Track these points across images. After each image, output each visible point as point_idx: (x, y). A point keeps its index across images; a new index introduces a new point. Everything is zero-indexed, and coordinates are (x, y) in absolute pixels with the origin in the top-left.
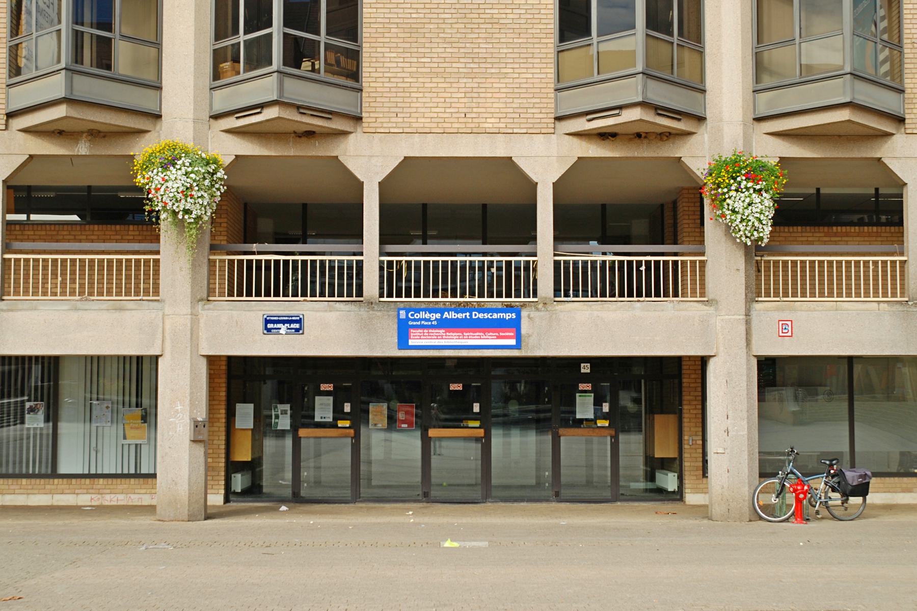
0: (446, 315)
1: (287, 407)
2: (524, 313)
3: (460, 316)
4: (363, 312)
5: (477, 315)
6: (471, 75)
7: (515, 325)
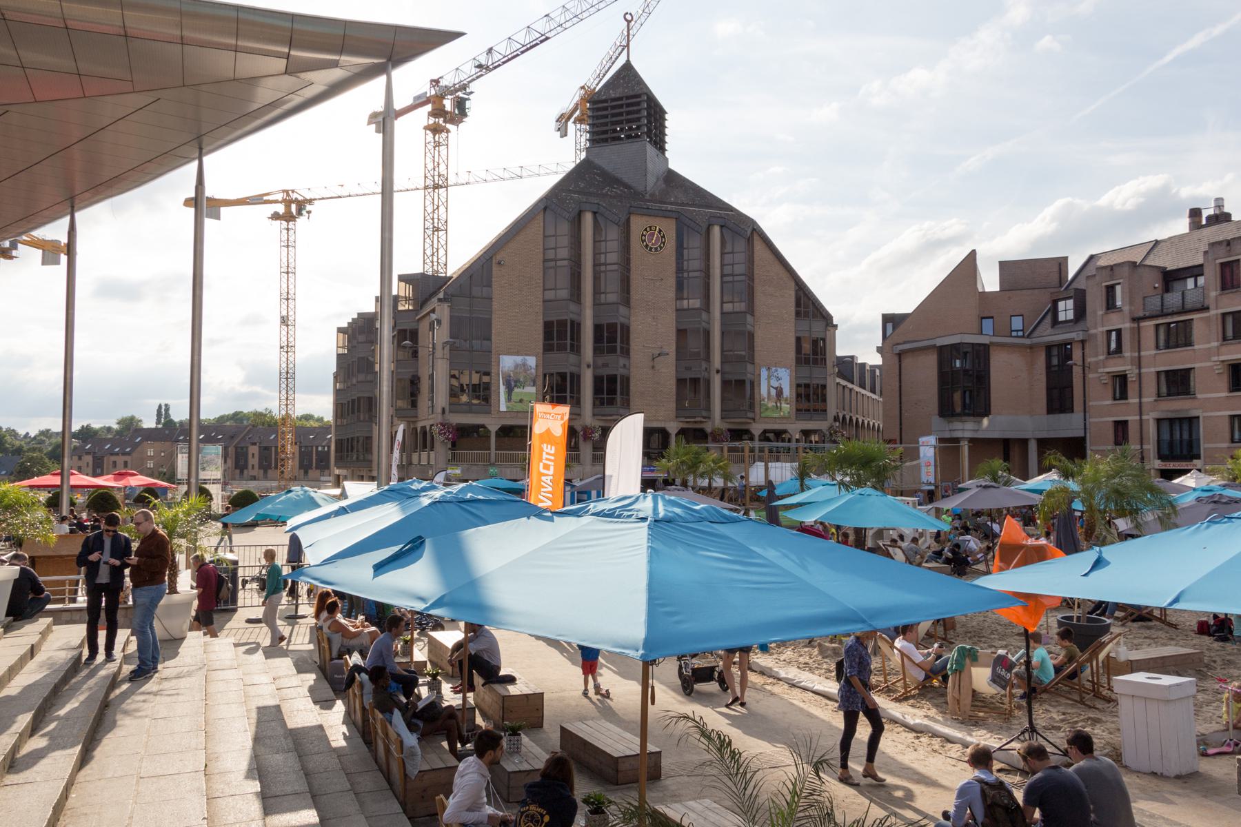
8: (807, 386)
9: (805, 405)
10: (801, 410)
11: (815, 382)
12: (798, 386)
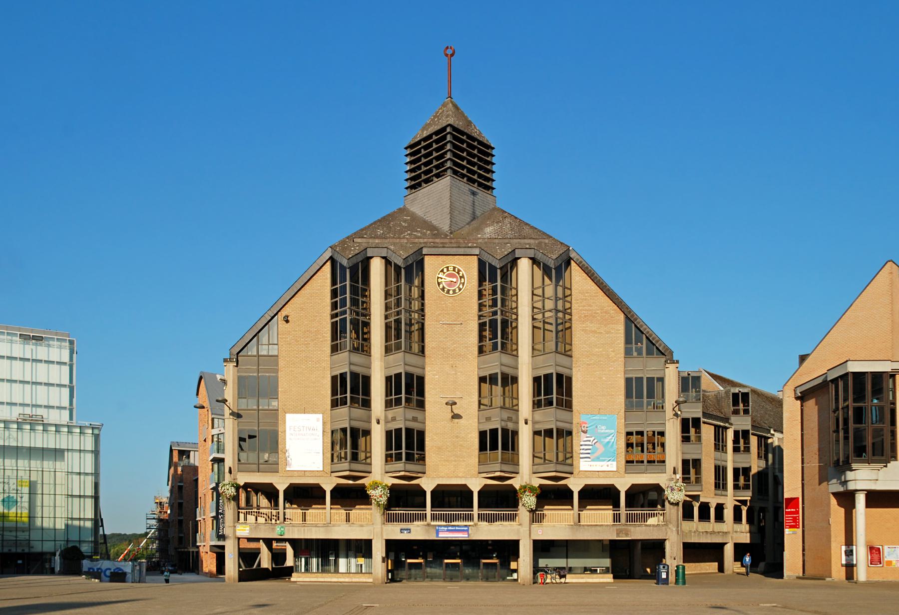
0: (449, 528)
1: (404, 553)
2: (470, 528)
5: (457, 528)
6: (455, 461)
7: (468, 531)
10: (632, 462)
12: (629, 434)
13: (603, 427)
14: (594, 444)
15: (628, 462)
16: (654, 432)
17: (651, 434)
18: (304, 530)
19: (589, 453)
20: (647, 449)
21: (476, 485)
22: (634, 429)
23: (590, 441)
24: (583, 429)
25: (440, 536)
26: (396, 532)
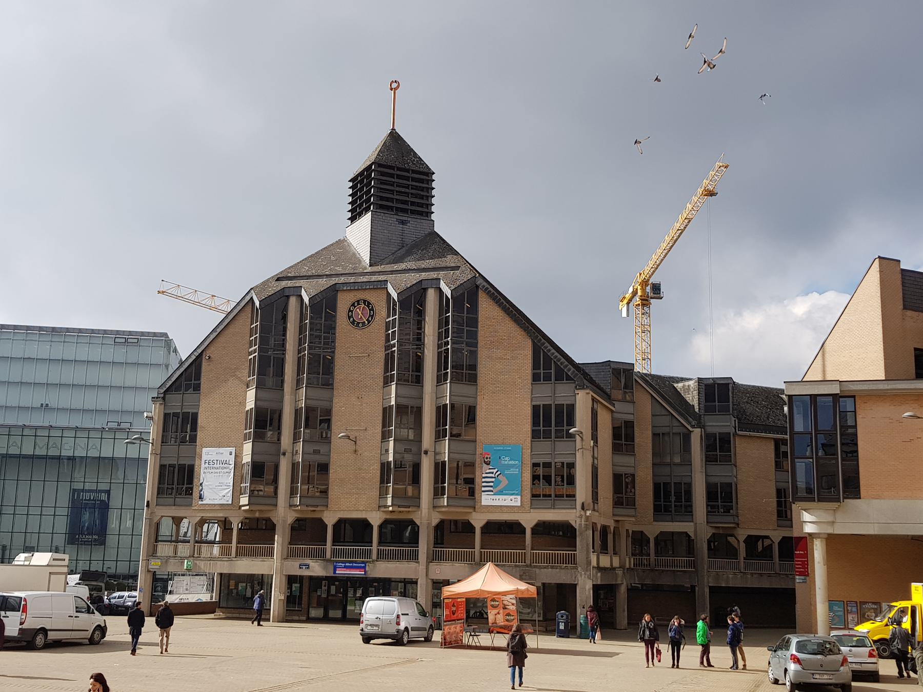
0: (346, 564)
2: (367, 564)
3: (350, 565)
4: (325, 563)
5: (354, 565)
7: (364, 567)
8: (547, 465)
9: (542, 488)
10: (539, 496)
11: (559, 460)
12: (535, 465)
13: (507, 458)
14: (497, 476)
15: (533, 496)
16: (563, 463)
17: (559, 465)
18: (210, 564)
19: (491, 487)
20: (556, 482)
21: (375, 519)
22: (541, 460)
23: (493, 473)
24: (486, 460)
25: (337, 572)
26: (294, 567)
